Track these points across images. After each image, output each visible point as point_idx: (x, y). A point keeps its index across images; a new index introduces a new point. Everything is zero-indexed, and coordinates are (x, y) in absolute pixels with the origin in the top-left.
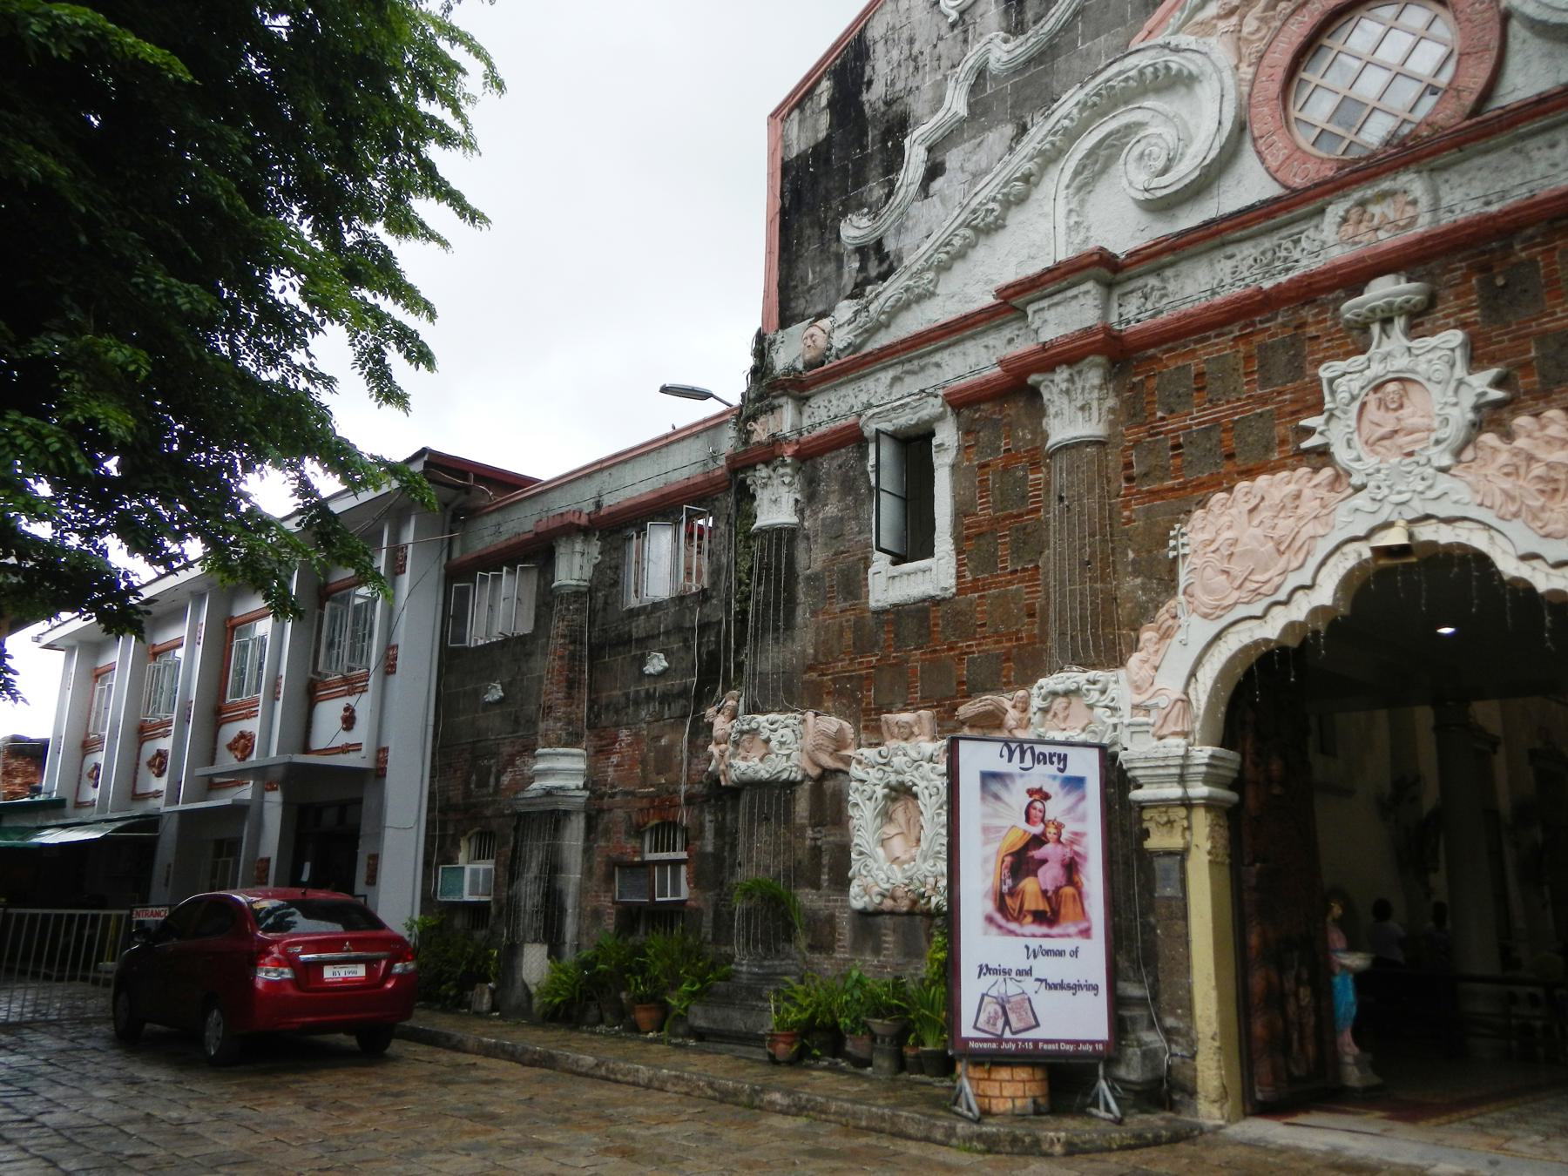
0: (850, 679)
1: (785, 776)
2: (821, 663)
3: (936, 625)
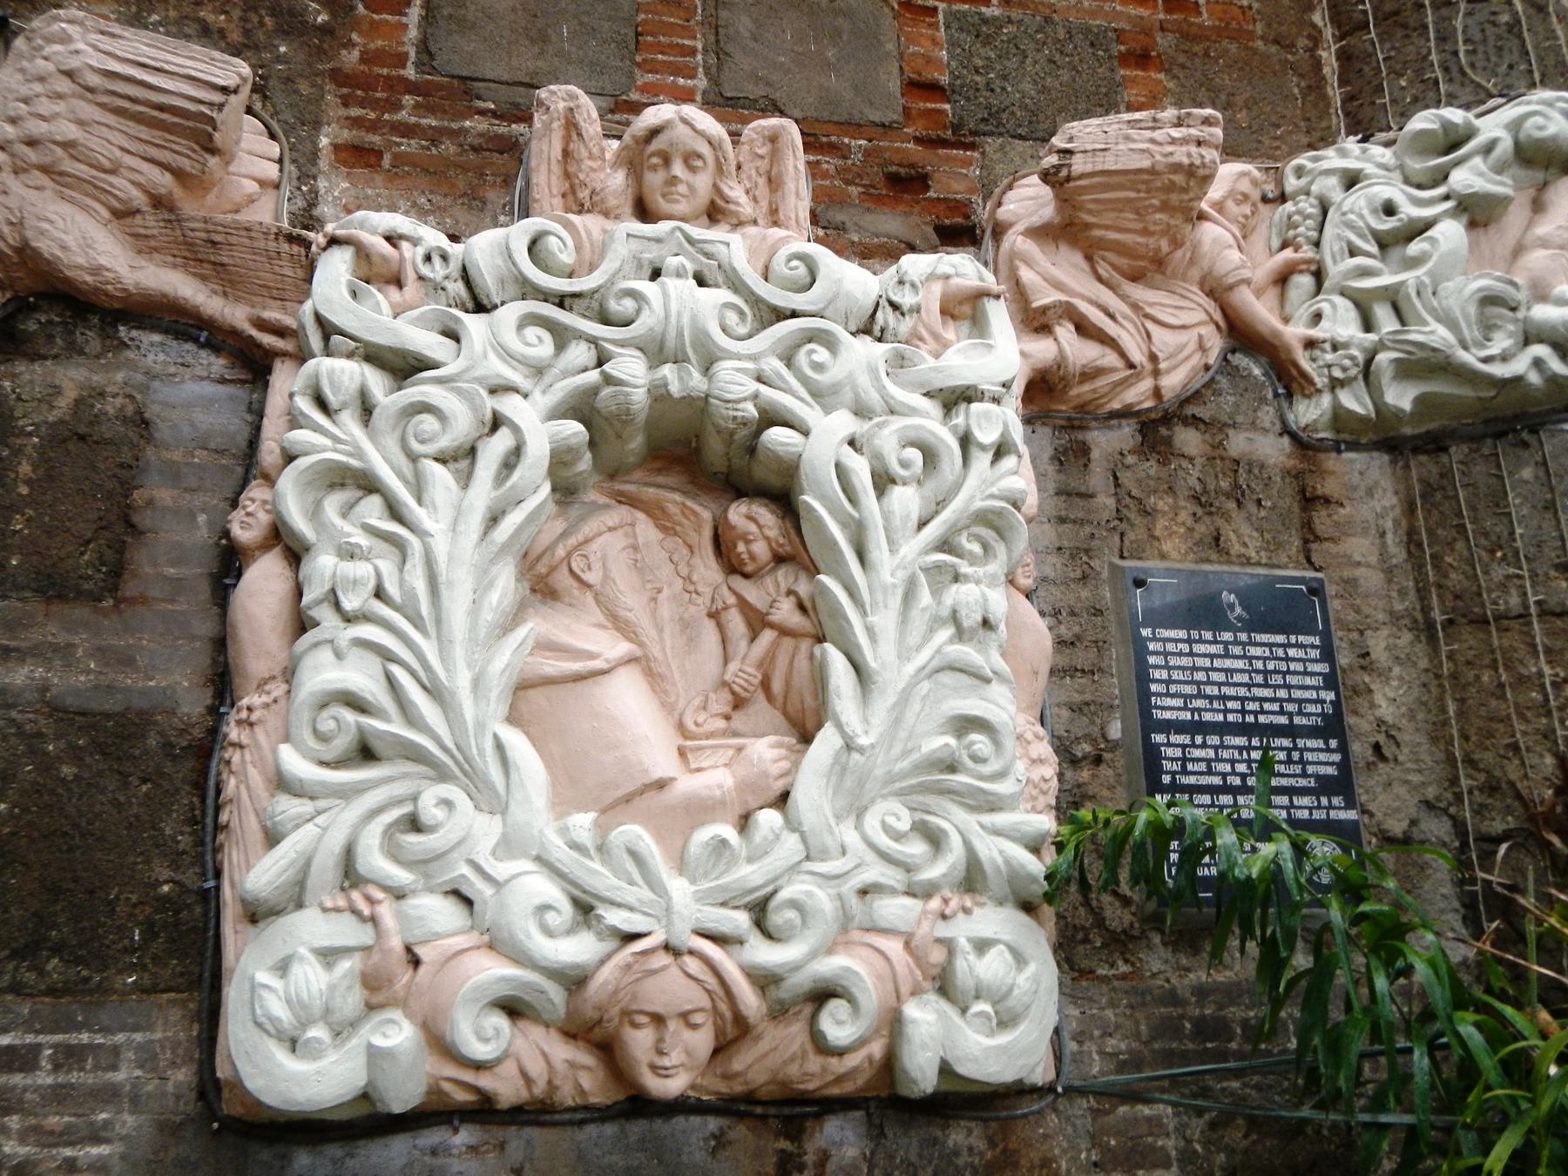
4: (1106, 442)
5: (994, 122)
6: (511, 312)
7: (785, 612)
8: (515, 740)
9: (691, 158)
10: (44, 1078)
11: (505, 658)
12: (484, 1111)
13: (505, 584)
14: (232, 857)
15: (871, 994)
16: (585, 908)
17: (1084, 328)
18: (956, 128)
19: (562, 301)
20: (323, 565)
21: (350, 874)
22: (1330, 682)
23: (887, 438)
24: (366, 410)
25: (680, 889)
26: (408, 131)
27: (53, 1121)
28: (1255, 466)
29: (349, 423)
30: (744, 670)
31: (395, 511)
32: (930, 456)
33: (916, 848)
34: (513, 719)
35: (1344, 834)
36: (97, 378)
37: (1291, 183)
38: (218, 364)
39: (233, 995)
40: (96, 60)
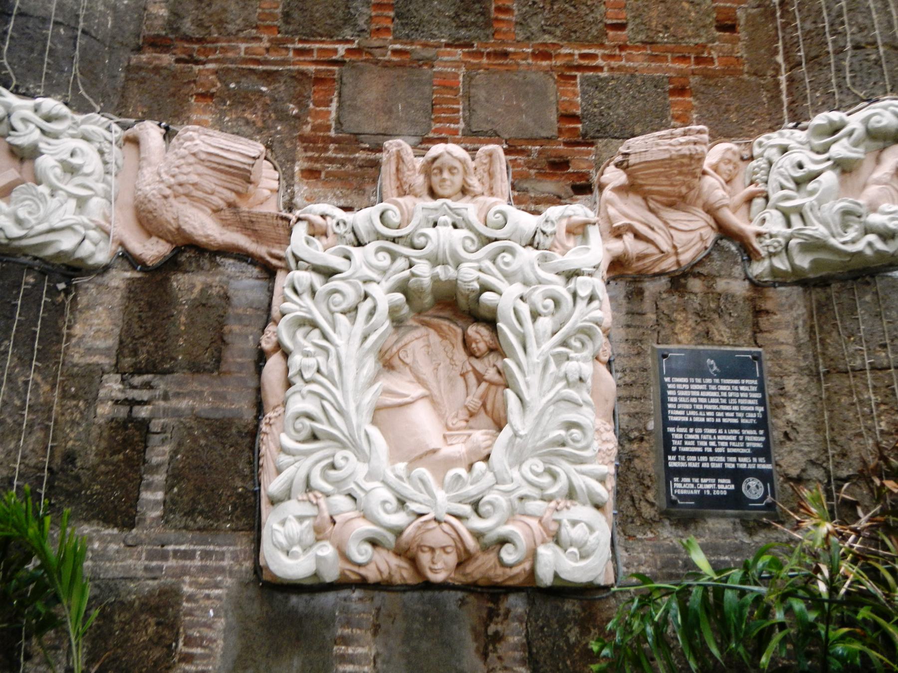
0: (269, 76)
1: (66, 243)
2: (189, 39)
3: (507, 10)
4: (651, 288)
5: (603, 132)
6: (372, 247)
7: (491, 374)
8: (374, 432)
9: (451, 170)
10: (197, 562)
11: (369, 398)
12: (363, 584)
13: (370, 365)
14: (264, 478)
15: (523, 541)
16: (402, 502)
17: (638, 236)
18: (584, 136)
19: (394, 240)
20: (296, 359)
21: (308, 487)
22: (762, 402)
23: (537, 296)
24: (313, 292)
25: (441, 495)
26: (331, 161)
27: (202, 580)
28: (728, 296)
29: (307, 300)
30: (474, 401)
31: (325, 336)
32: (557, 303)
33: (546, 480)
34: (374, 422)
35: (765, 477)
36: (209, 280)
37: (757, 151)
38: (256, 271)
39: (265, 532)
40: (204, 148)
